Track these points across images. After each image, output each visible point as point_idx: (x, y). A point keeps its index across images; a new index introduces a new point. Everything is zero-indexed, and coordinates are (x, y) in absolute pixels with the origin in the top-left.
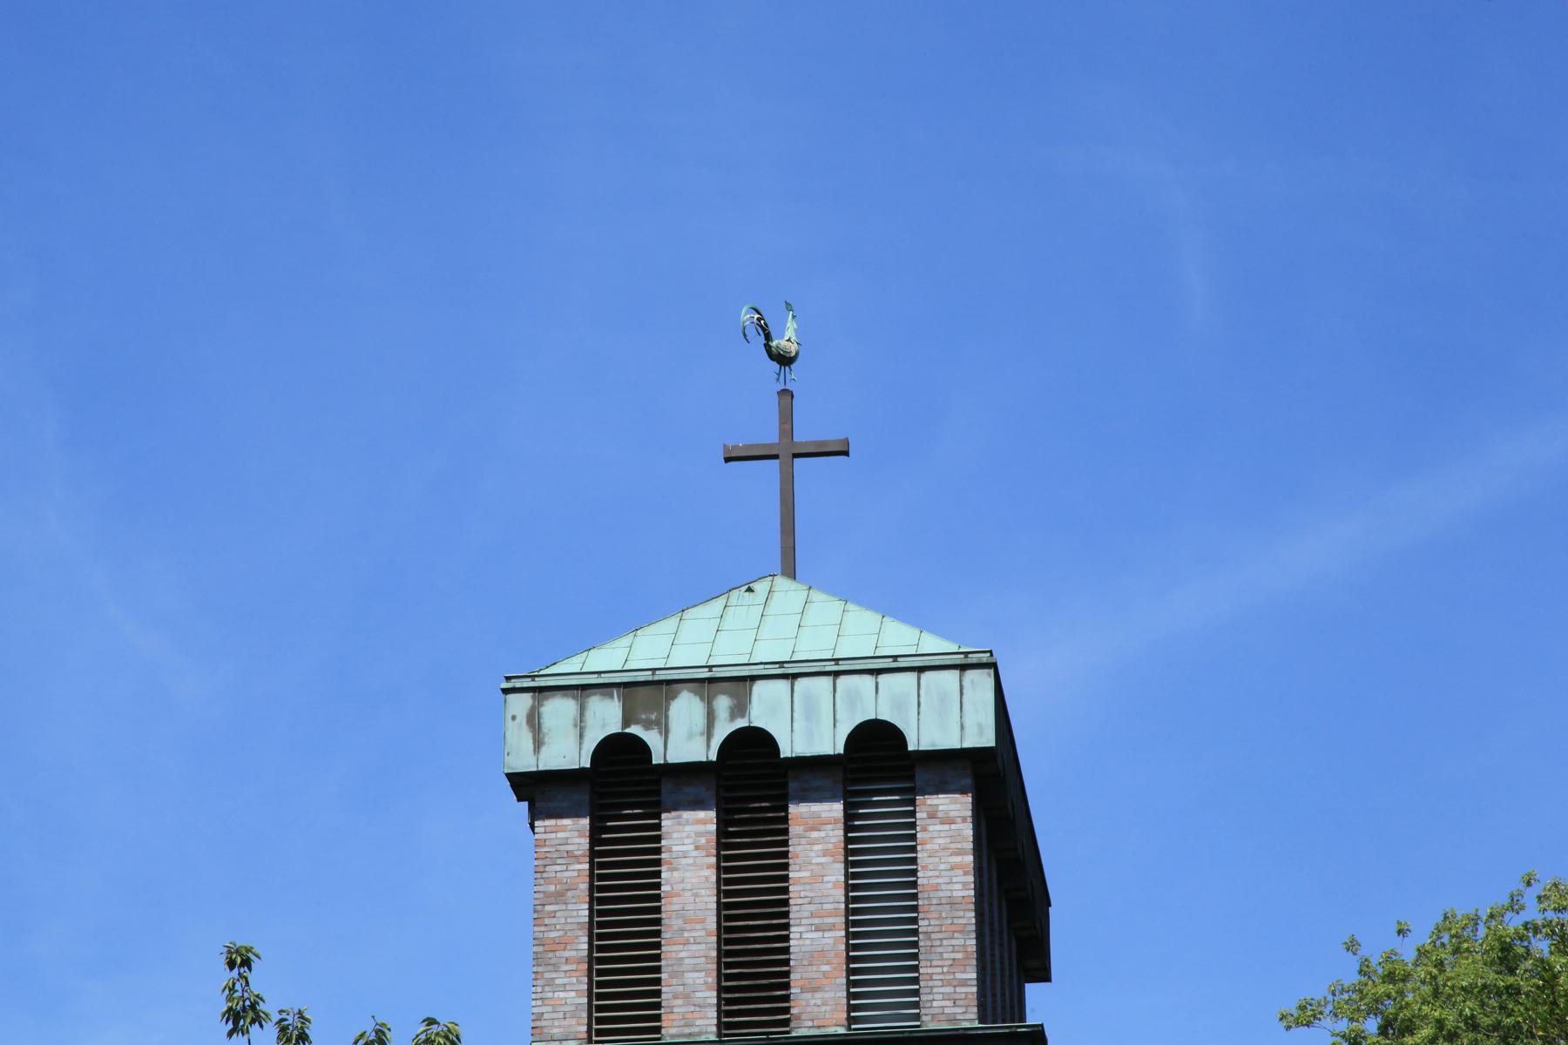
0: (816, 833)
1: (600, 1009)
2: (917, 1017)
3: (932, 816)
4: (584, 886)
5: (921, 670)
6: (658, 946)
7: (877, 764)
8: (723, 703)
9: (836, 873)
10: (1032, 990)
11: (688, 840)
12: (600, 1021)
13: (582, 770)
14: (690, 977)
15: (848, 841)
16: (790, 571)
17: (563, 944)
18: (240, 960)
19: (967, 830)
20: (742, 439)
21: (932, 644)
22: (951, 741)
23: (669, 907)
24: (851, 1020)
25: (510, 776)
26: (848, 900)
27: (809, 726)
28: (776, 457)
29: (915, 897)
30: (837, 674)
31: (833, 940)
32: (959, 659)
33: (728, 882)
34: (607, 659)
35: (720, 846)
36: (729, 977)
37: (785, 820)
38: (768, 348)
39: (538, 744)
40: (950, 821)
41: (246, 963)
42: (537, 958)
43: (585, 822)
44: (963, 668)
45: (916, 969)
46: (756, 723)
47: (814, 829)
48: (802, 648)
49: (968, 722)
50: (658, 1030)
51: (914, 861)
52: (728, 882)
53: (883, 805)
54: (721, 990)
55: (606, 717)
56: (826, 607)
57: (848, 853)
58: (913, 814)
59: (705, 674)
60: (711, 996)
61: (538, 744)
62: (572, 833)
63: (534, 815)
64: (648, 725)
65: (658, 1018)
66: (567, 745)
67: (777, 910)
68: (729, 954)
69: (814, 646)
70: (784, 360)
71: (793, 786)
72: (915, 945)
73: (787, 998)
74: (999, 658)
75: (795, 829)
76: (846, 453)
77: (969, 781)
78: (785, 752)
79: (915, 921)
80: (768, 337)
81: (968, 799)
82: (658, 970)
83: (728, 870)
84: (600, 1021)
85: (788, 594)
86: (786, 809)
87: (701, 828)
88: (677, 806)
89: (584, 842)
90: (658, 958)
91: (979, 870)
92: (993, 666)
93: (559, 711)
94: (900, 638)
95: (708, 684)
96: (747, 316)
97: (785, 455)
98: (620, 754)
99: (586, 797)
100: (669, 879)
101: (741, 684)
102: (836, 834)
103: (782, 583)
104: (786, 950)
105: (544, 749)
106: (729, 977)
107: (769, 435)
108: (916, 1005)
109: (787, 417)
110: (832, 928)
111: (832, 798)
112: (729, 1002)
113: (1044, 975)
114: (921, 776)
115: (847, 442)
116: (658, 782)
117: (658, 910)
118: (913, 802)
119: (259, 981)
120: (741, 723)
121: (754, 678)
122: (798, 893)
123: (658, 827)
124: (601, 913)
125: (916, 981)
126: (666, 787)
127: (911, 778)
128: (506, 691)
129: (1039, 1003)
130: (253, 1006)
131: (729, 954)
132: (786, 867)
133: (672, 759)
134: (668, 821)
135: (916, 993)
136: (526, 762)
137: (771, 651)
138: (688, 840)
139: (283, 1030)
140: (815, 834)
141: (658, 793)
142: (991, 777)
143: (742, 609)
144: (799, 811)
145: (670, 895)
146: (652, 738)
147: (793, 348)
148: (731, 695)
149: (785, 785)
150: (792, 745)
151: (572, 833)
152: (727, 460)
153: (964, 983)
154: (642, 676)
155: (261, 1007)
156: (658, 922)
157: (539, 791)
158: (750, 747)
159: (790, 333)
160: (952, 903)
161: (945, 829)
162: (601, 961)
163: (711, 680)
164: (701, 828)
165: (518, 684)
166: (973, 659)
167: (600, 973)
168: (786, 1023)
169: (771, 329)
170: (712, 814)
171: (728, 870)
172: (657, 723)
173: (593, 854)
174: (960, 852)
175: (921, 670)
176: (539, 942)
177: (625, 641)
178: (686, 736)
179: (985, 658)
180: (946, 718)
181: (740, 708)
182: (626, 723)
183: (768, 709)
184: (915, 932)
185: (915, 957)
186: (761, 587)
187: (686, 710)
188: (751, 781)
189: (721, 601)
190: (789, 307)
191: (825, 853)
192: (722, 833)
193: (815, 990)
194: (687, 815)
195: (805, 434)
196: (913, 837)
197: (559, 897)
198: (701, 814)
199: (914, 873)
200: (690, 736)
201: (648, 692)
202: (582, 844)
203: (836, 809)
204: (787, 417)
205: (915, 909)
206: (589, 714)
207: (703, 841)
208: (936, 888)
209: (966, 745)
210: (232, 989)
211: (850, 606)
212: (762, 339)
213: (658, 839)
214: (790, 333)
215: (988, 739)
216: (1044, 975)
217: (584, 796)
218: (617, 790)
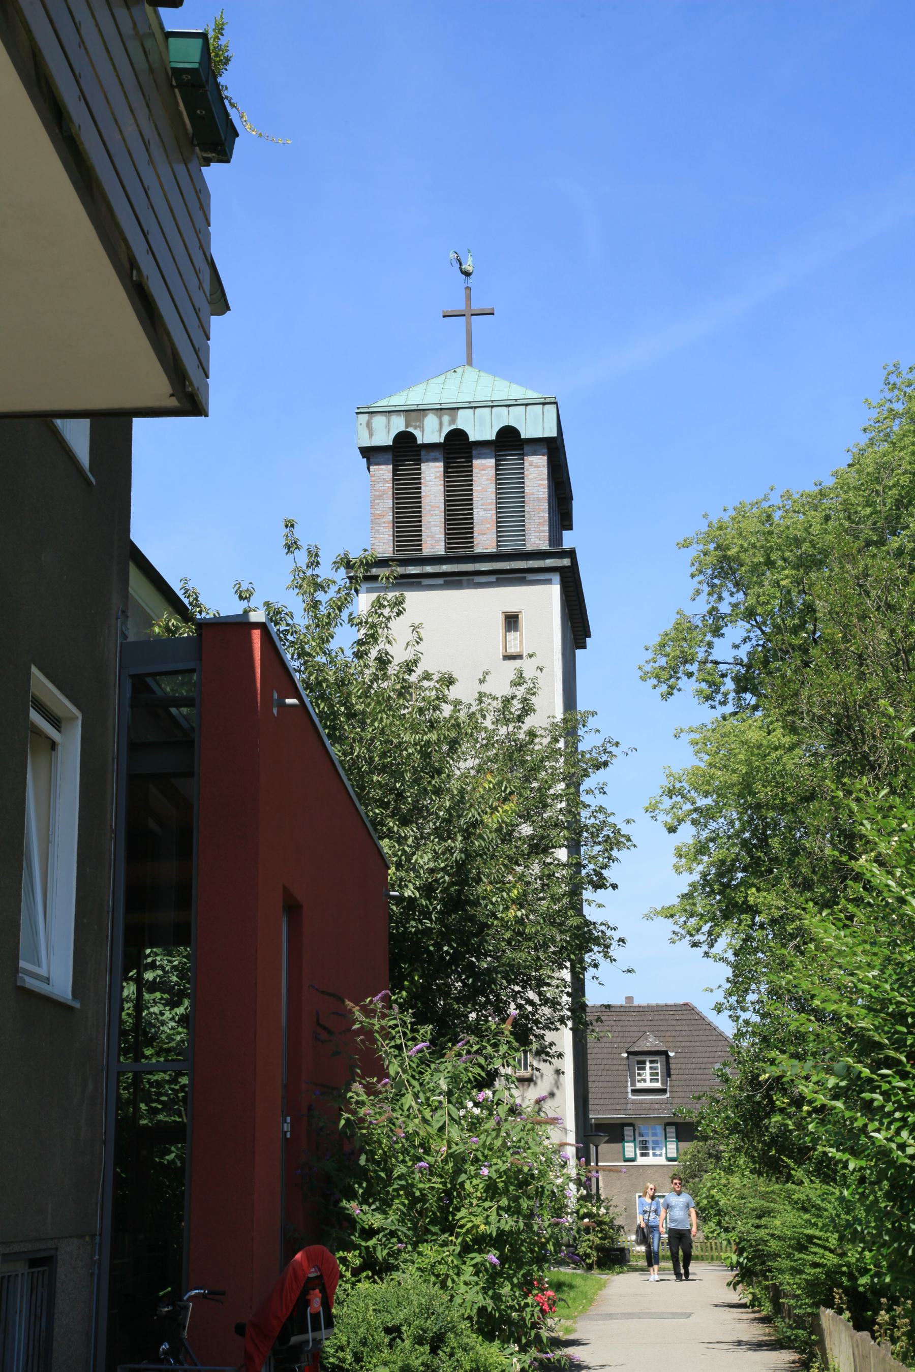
0: (484, 470)
1: (397, 541)
2: (524, 545)
3: (531, 465)
4: (391, 493)
5: (527, 405)
6: (420, 517)
7: (509, 442)
8: (446, 419)
9: (492, 488)
10: (566, 534)
11: (432, 474)
12: (397, 546)
13: (389, 446)
14: (433, 529)
15: (497, 475)
16: (470, 363)
17: (383, 516)
18: (290, 525)
19: (545, 470)
20: (449, 309)
21: (531, 394)
22: (538, 434)
23: (425, 501)
24: (498, 546)
25: (360, 448)
26: (497, 498)
27: (481, 428)
28: (464, 315)
29: (523, 497)
30: (492, 407)
31: (491, 514)
32: (542, 401)
33: (448, 491)
34: (398, 400)
35: (445, 477)
36: (449, 529)
37: (471, 466)
38: (461, 268)
39: (371, 435)
40: (538, 467)
41: (292, 526)
42: (372, 521)
43: (390, 467)
44: (544, 404)
45: (524, 526)
46: (459, 427)
47: (483, 470)
48: (476, 395)
49: (546, 427)
50: (421, 550)
51: (523, 483)
52: (448, 491)
53: (511, 460)
54: (446, 534)
55: (399, 424)
56: (486, 379)
57: (497, 479)
58: (523, 464)
59: (438, 406)
60: (442, 537)
61: (371, 435)
62: (385, 471)
63: (369, 464)
64: (415, 428)
65: (421, 545)
66: (383, 435)
67: (468, 502)
68: (449, 520)
69: (483, 395)
70: (467, 274)
71: (474, 452)
72: (523, 516)
73: (472, 538)
74: (557, 400)
75: (475, 470)
76: (493, 314)
77: (546, 451)
78: (472, 438)
79: (523, 507)
80: (461, 264)
81: (545, 458)
82: (420, 526)
83: (448, 486)
84: (397, 546)
85: (471, 373)
86: (471, 462)
87: (437, 470)
88: (427, 461)
89: (390, 475)
90: (420, 521)
91: (549, 486)
92: (556, 403)
93: (379, 421)
94: (518, 392)
95: (440, 411)
96: (452, 255)
97: (468, 315)
98: (405, 440)
99: (391, 457)
100: (424, 489)
101: (453, 410)
102: (492, 472)
103: (468, 368)
104: (472, 519)
105: (373, 437)
106: (449, 529)
107: (460, 306)
108: (524, 540)
109: (468, 298)
110: (491, 509)
111: (491, 458)
112: (449, 539)
113: (570, 527)
114: (527, 448)
115: (493, 309)
116: (420, 451)
117: (420, 502)
118: (523, 459)
119: (298, 533)
120: (453, 427)
121: (458, 408)
122: (476, 496)
123: (420, 469)
124: (397, 503)
125: (524, 530)
126: (423, 453)
127: (522, 449)
128: (357, 413)
129: (569, 540)
130: (295, 543)
131: (449, 520)
132: (471, 485)
133: (426, 442)
134: (424, 466)
135: (524, 535)
136: (367, 443)
137: (465, 397)
138: (432, 474)
139: (310, 552)
140: (483, 472)
141: (420, 455)
142: (553, 448)
143: (452, 380)
144: (476, 462)
145: (425, 496)
146: (417, 433)
147: (471, 269)
148: (450, 415)
149: (471, 452)
150: (474, 435)
151: (385, 471)
152: (444, 316)
153: (543, 531)
154: (414, 407)
155: (299, 543)
156: (420, 507)
157: (370, 454)
158: (457, 438)
159: (469, 262)
160: (539, 500)
161: (536, 469)
162: (397, 522)
163: (441, 409)
164: (437, 470)
165: (362, 410)
166: (548, 400)
167: (397, 527)
168: (472, 547)
169: (462, 261)
170: (442, 464)
171: (448, 486)
172: (419, 427)
173: (394, 480)
174: (542, 479)
175: (527, 405)
176: (373, 515)
177: (405, 393)
178: (431, 432)
179: (553, 400)
180: (535, 425)
181: (453, 421)
182: (407, 426)
183: (467, 423)
184: (523, 511)
185: (524, 521)
186: (459, 370)
187: (431, 421)
188: (457, 450)
189: (443, 377)
190: (469, 251)
191: (488, 480)
192: (446, 472)
193: (484, 534)
194: (432, 464)
195: (476, 306)
196: (523, 473)
197: (380, 497)
198: (437, 464)
199: (523, 487)
200: (433, 432)
201: (416, 413)
202: (389, 476)
203: (492, 462)
204: (468, 298)
205: (523, 502)
206: (391, 423)
207: (438, 475)
208: (533, 494)
209: (545, 436)
210: (287, 536)
211: (497, 379)
212: (458, 265)
213: (420, 474)
214: (469, 262)
215: (554, 434)
216: (570, 527)
217: (389, 456)
218: (404, 452)
